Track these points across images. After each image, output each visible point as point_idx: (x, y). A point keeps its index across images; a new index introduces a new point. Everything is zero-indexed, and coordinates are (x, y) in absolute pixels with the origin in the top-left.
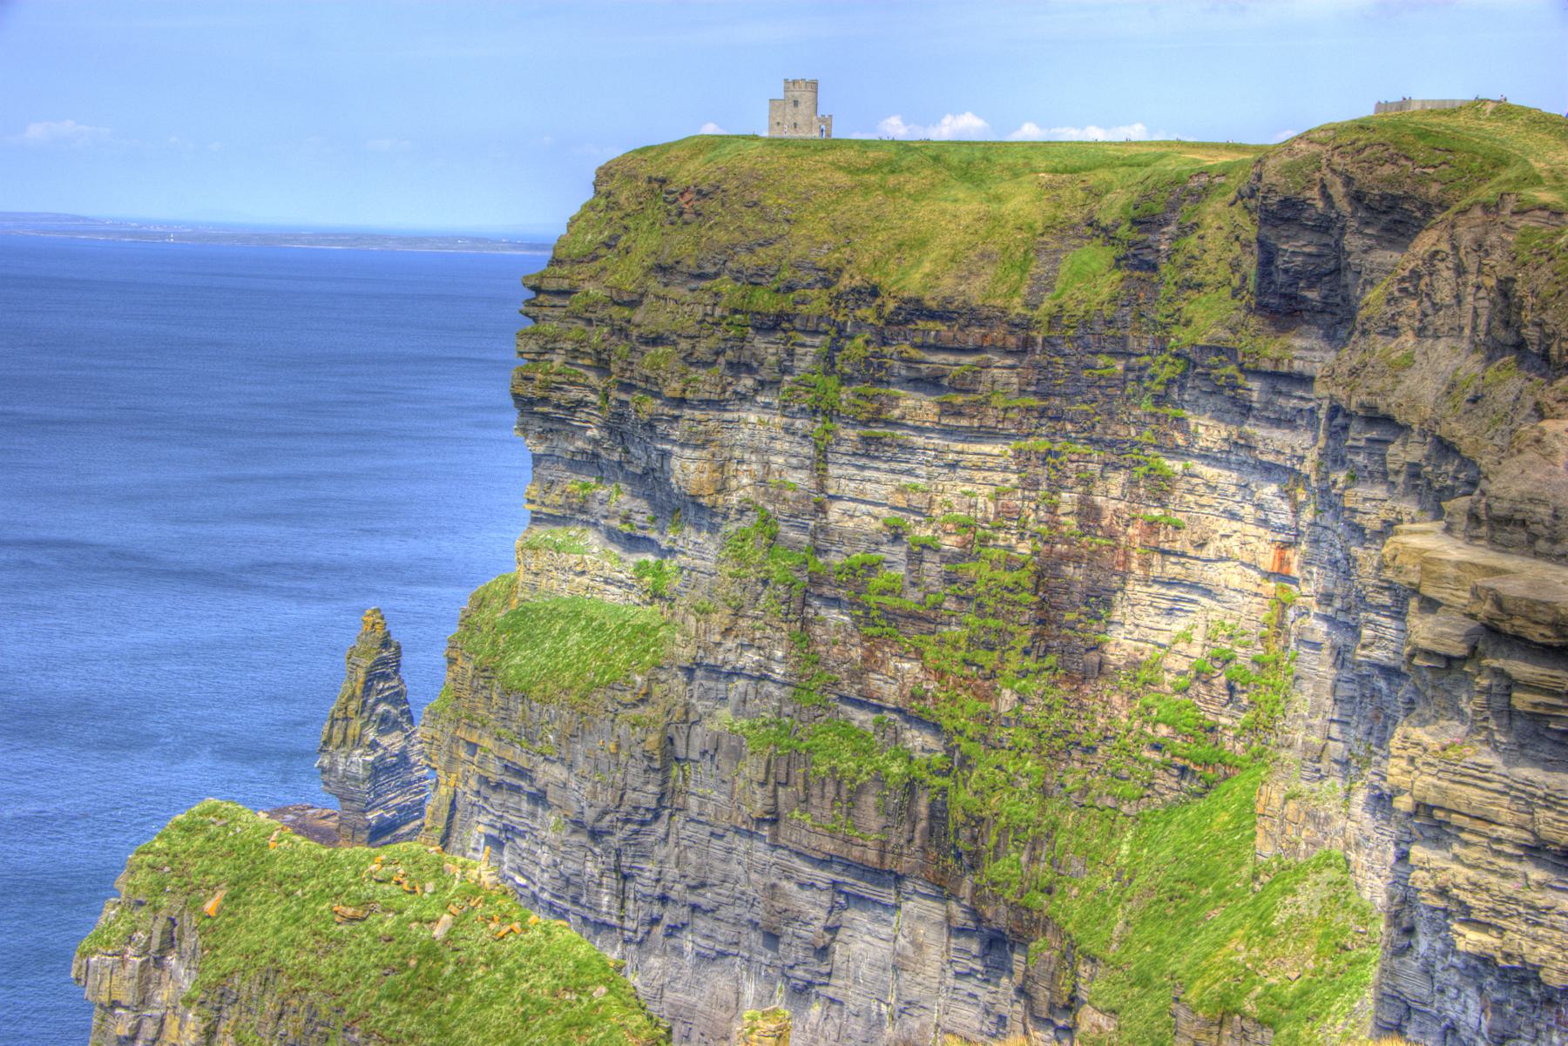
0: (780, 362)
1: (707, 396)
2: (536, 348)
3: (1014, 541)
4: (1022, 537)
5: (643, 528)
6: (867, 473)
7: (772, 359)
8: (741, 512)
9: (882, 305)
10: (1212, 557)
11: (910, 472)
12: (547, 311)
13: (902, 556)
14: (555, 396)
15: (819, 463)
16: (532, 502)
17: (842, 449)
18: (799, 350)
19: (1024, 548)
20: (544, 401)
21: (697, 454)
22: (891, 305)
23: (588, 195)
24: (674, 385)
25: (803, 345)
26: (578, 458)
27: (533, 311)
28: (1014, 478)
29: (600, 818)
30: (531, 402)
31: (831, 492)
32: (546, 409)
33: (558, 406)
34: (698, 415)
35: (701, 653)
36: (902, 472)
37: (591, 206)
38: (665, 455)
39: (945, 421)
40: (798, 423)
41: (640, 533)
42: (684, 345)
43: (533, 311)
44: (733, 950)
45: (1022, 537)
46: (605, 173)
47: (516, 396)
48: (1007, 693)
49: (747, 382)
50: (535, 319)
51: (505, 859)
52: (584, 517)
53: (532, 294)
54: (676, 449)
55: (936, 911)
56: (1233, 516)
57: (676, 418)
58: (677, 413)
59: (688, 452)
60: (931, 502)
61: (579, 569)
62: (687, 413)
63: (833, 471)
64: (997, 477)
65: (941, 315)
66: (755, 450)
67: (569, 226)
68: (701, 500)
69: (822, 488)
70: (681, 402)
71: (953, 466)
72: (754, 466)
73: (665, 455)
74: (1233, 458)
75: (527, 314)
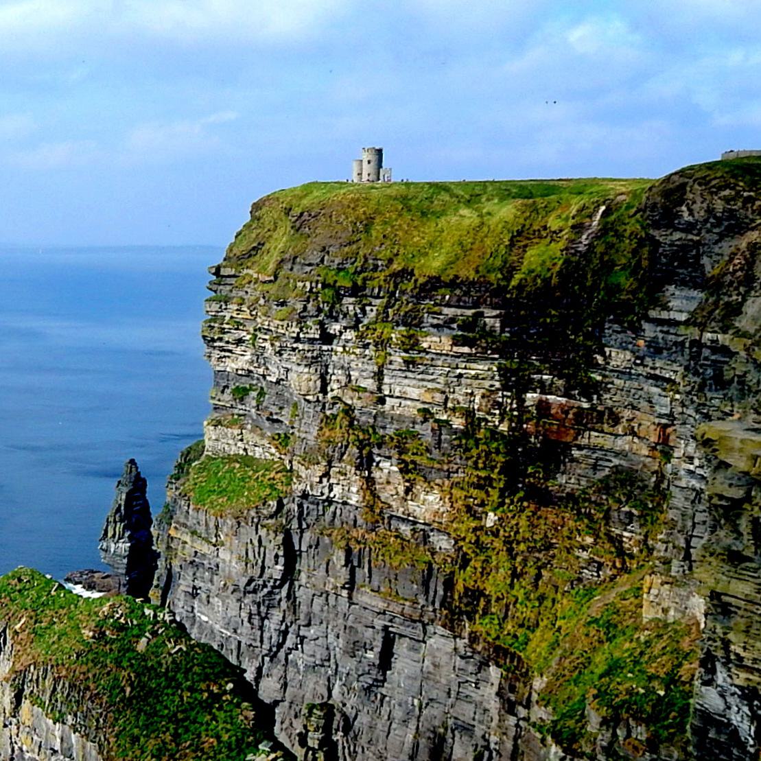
0: (356, 314)
1: (312, 336)
2: (217, 309)
3: (497, 423)
4: (501, 422)
5: (276, 414)
6: (406, 381)
7: (352, 313)
8: (334, 404)
9: (416, 281)
10: (620, 433)
11: (433, 380)
12: (221, 287)
13: (429, 431)
14: (226, 337)
15: (379, 376)
16: (213, 398)
17: (392, 367)
18: (368, 308)
19: (504, 427)
20: (220, 339)
21: (306, 370)
22: (421, 280)
23: (248, 218)
24: (293, 329)
25: (370, 304)
26: (240, 372)
27: (215, 287)
28: (498, 385)
29: (249, 583)
30: (213, 340)
31: (387, 393)
32: (221, 344)
33: (228, 342)
34: (306, 347)
35: (308, 488)
36: (429, 381)
37: (247, 226)
38: (288, 370)
39: (455, 349)
40: (367, 352)
41: (275, 417)
42: (299, 307)
43: (215, 287)
44: (326, 664)
45: (501, 422)
46: (257, 207)
47: (204, 337)
48: (491, 514)
49: (335, 328)
50: (215, 292)
51: (196, 606)
52: (243, 407)
53: (214, 278)
54: (295, 368)
55: (449, 645)
56: (634, 408)
57: (294, 349)
58: (295, 345)
59: (301, 369)
60: (447, 399)
61: (240, 437)
62: (301, 346)
63: (386, 380)
64: (487, 384)
65: (453, 284)
66: (342, 367)
67: (236, 237)
68: (308, 397)
69: (380, 390)
70: (297, 340)
71: (460, 376)
72: (339, 378)
73: (288, 370)
74: (633, 371)
75: (211, 289)
